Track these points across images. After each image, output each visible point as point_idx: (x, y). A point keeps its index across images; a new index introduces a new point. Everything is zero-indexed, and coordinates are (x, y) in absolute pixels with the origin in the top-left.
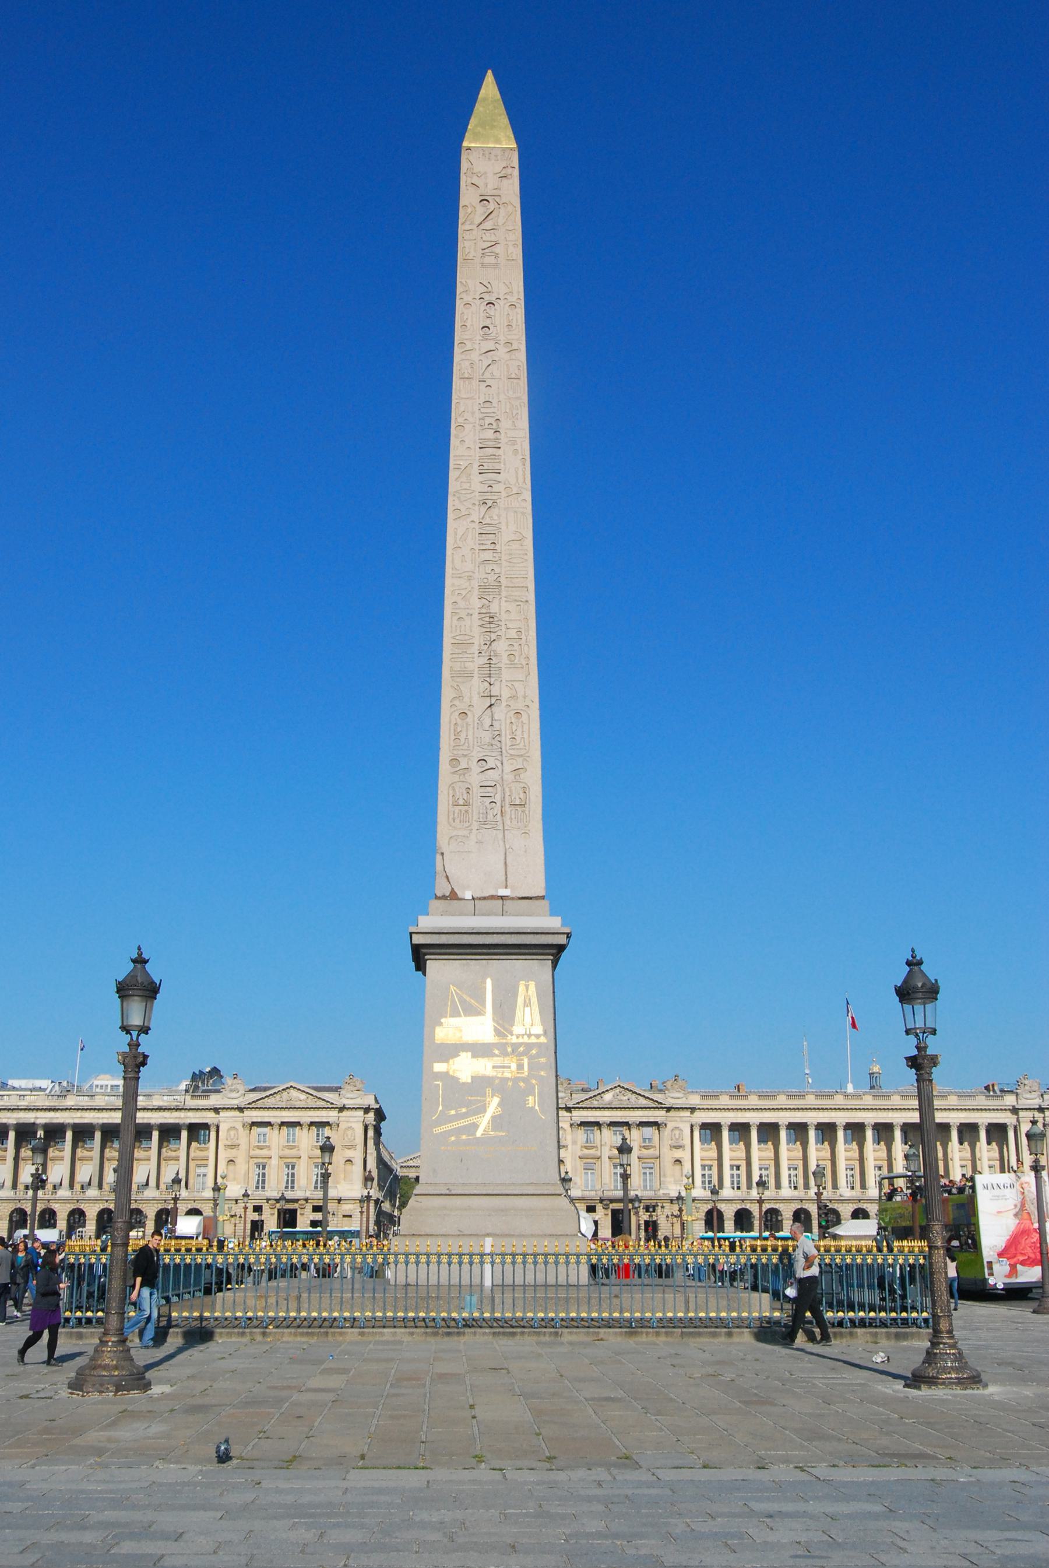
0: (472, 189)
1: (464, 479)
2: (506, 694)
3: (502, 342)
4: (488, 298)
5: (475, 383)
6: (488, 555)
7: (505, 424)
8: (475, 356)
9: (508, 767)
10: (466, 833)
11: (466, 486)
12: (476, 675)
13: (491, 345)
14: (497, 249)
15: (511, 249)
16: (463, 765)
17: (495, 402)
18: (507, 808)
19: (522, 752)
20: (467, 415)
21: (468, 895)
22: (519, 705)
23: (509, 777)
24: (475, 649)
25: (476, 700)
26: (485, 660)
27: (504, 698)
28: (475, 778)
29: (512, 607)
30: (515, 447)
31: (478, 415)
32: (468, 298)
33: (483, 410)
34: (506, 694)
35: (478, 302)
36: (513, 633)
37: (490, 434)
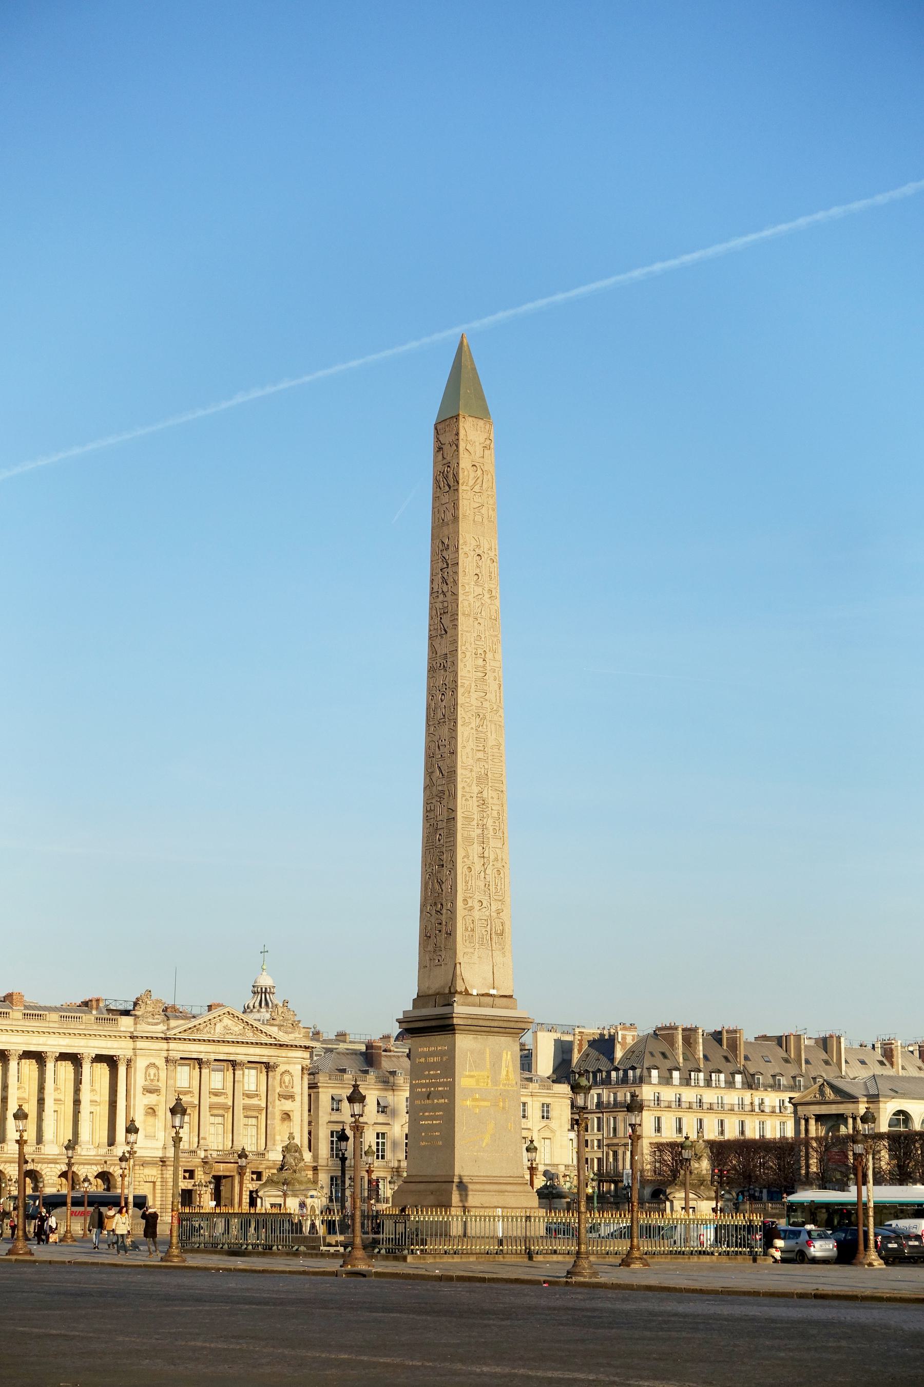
0: (466, 453)
1: (466, 695)
2: (492, 857)
3: (486, 589)
4: (478, 552)
5: (471, 619)
6: (480, 755)
7: (489, 656)
8: (471, 598)
9: (494, 908)
10: (472, 950)
11: (468, 700)
12: (476, 841)
13: (479, 590)
14: (484, 511)
15: (491, 512)
16: (470, 904)
17: (483, 636)
18: (493, 936)
19: (501, 898)
20: (468, 645)
21: (475, 993)
22: (499, 865)
23: (494, 914)
24: (475, 823)
25: (476, 859)
26: (480, 831)
27: (491, 860)
28: (476, 914)
29: (495, 794)
30: (496, 674)
31: (473, 646)
32: (466, 549)
33: (477, 642)
34: (492, 857)
35: (472, 553)
36: (495, 814)
37: (480, 662)
